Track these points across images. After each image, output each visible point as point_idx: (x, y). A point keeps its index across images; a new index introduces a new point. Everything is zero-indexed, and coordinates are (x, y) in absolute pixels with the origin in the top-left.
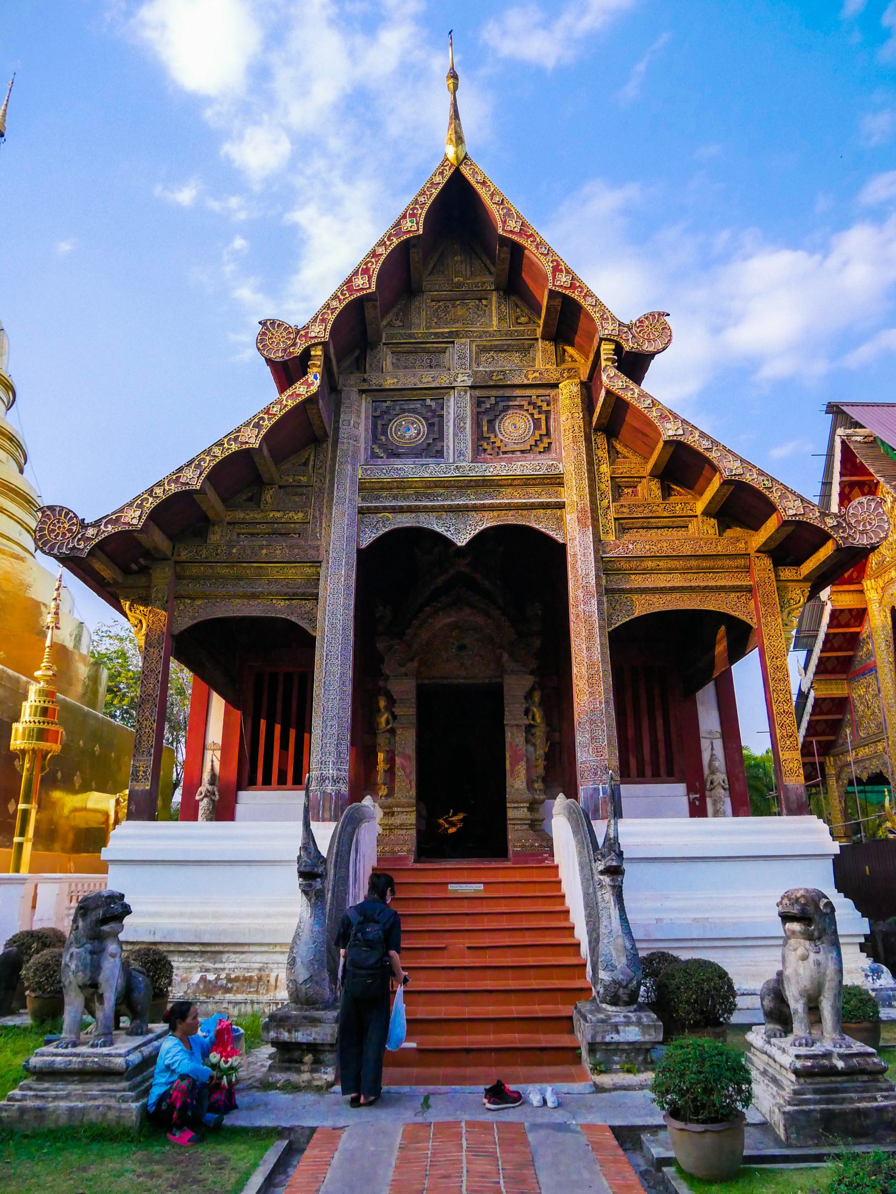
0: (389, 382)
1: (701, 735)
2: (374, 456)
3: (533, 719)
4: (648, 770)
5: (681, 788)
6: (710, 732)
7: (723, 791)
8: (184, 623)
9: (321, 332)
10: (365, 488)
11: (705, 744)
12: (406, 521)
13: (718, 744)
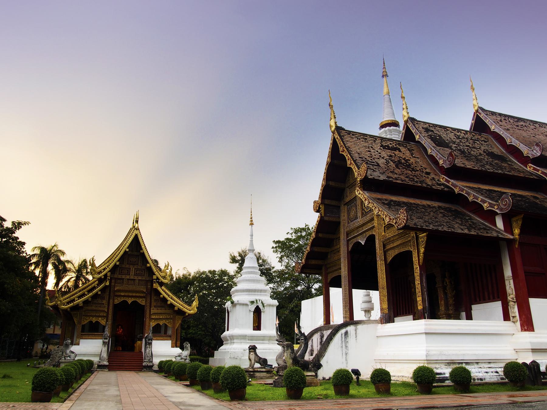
0: (348, 199)
1: (506, 278)
2: (349, 223)
3: (446, 283)
4: (491, 297)
5: (500, 303)
6: (508, 277)
7: (513, 303)
8: (329, 280)
9: (320, 201)
10: (348, 234)
11: (507, 283)
12: (355, 241)
13: (512, 281)
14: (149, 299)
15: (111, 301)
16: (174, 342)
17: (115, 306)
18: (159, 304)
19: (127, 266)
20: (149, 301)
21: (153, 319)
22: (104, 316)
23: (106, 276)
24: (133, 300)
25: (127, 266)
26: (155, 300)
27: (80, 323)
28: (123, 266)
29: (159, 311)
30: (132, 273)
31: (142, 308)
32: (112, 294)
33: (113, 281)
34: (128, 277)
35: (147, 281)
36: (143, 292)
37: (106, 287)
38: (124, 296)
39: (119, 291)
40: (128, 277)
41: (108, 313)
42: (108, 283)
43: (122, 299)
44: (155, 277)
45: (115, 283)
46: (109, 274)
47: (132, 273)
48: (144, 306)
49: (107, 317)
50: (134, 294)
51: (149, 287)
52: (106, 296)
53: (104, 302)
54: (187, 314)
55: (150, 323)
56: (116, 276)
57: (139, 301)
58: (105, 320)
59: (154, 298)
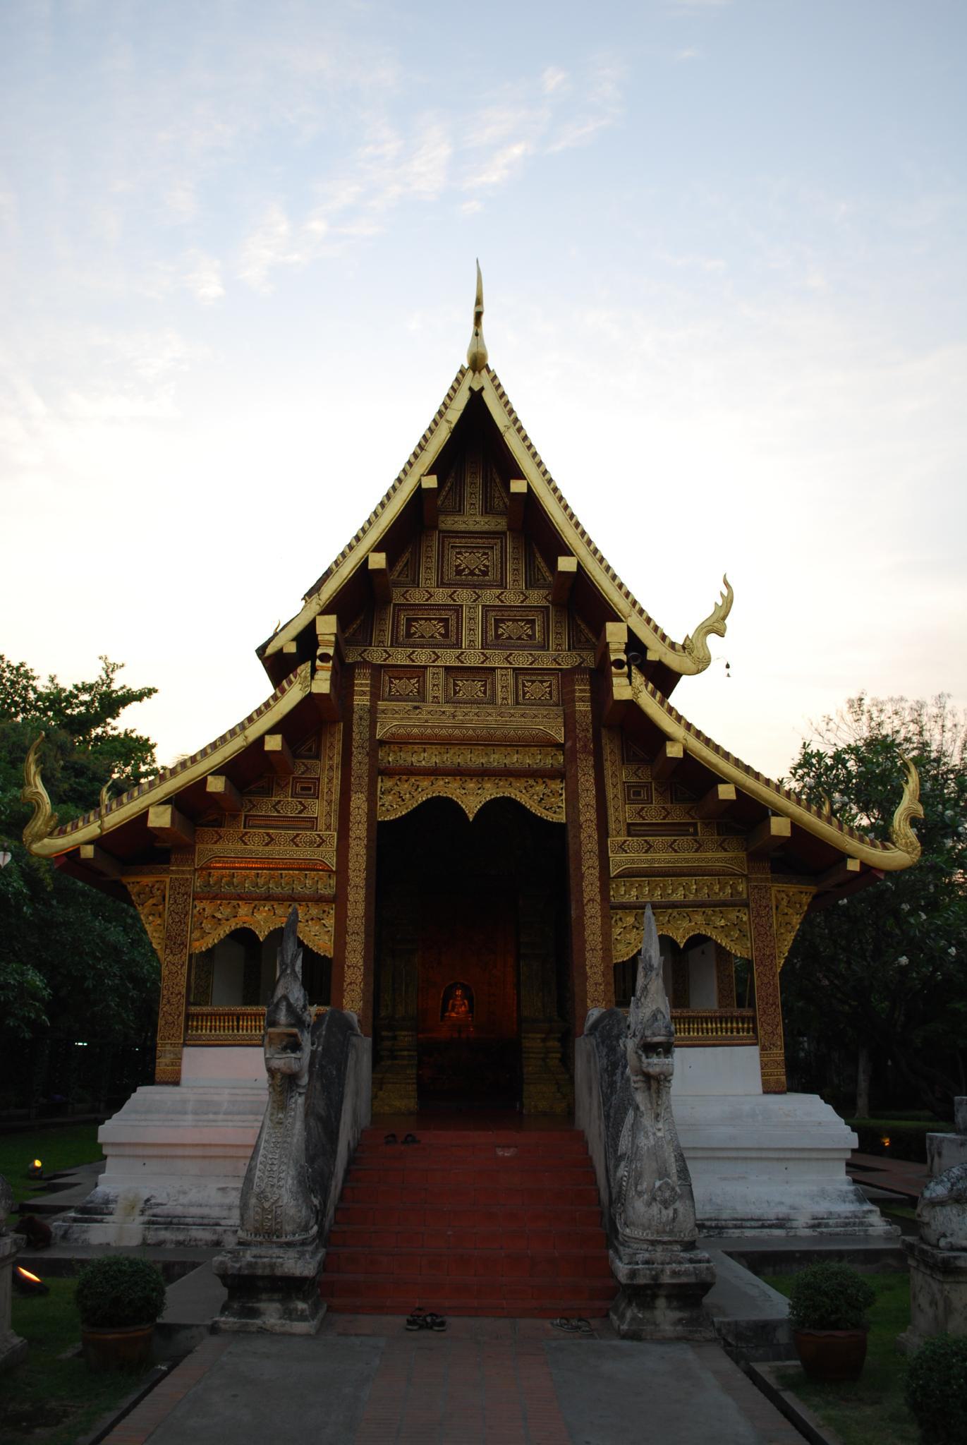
14: (587, 782)
15: (359, 802)
16: (779, 1053)
17: (386, 837)
18: (653, 814)
19: (441, 596)
20: (588, 797)
21: (625, 907)
22: (319, 899)
23: (307, 638)
24: (491, 791)
25: (441, 596)
26: (628, 787)
27: (175, 941)
28: (417, 597)
29: (662, 858)
30: (472, 631)
31: (552, 842)
32: (359, 760)
33: (362, 683)
34: (449, 658)
35: (566, 676)
36: (547, 744)
37: (310, 700)
38: (434, 772)
39: (399, 742)
40: (449, 658)
41: (342, 872)
42: (322, 685)
43: (427, 790)
44: (615, 634)
45: (375, 695)
46: (327, 627)
47: (472, 631)
48: (561, 827)
49: (339, 900)
50: (496, 759)
51: (583, 707)
52: (328, 773)
53: (317, 808)
54: (853, 866)
55: (606, 935)
56: (376, 655)
57: (529, 797)
58: (330, 922)
59: (618, 777)
